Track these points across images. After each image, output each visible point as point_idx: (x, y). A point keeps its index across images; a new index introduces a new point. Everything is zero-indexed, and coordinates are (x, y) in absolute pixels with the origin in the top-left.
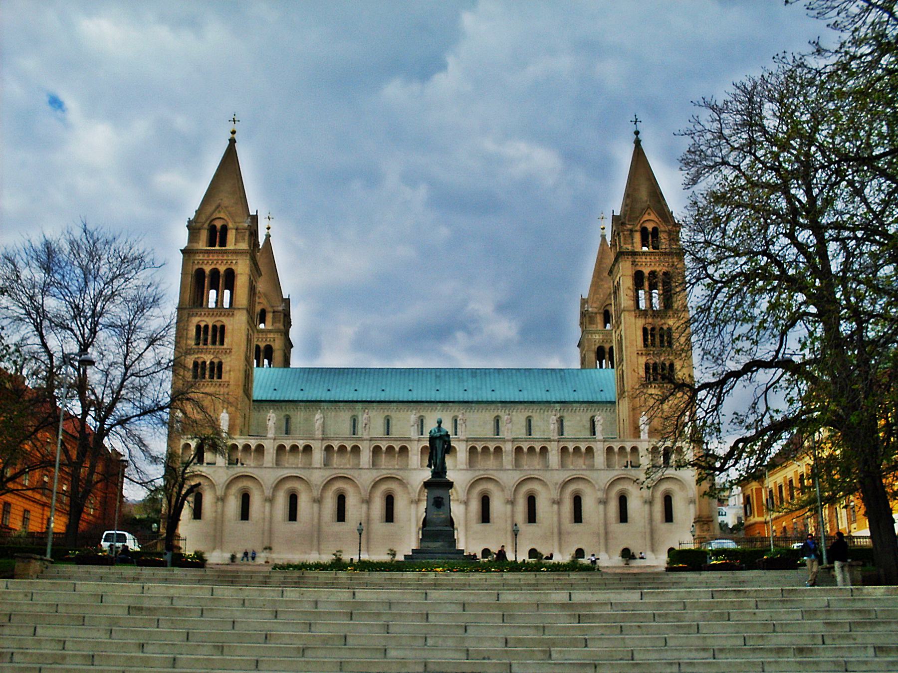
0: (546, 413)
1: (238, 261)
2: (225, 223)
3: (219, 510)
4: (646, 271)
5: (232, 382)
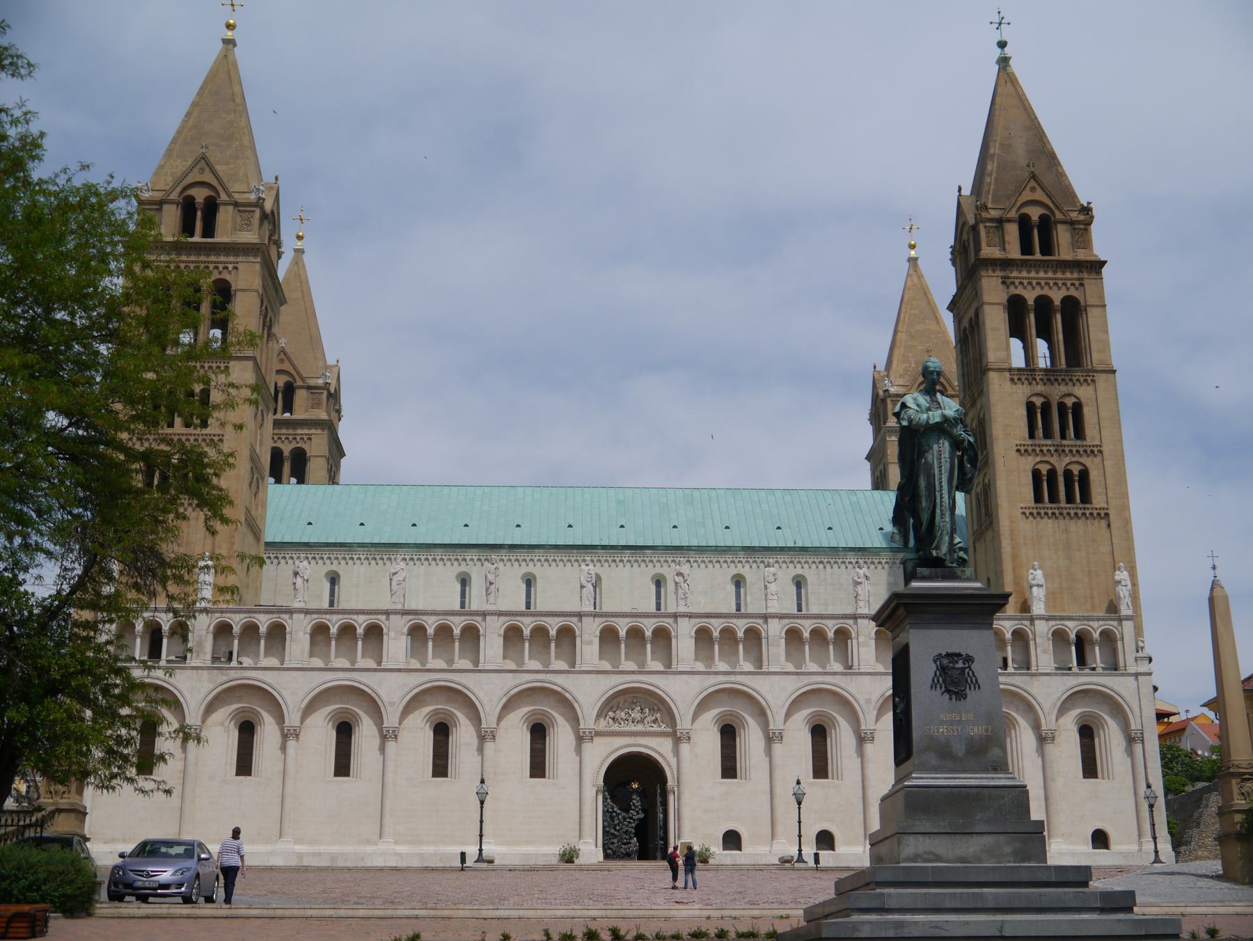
4: (1030, 296)
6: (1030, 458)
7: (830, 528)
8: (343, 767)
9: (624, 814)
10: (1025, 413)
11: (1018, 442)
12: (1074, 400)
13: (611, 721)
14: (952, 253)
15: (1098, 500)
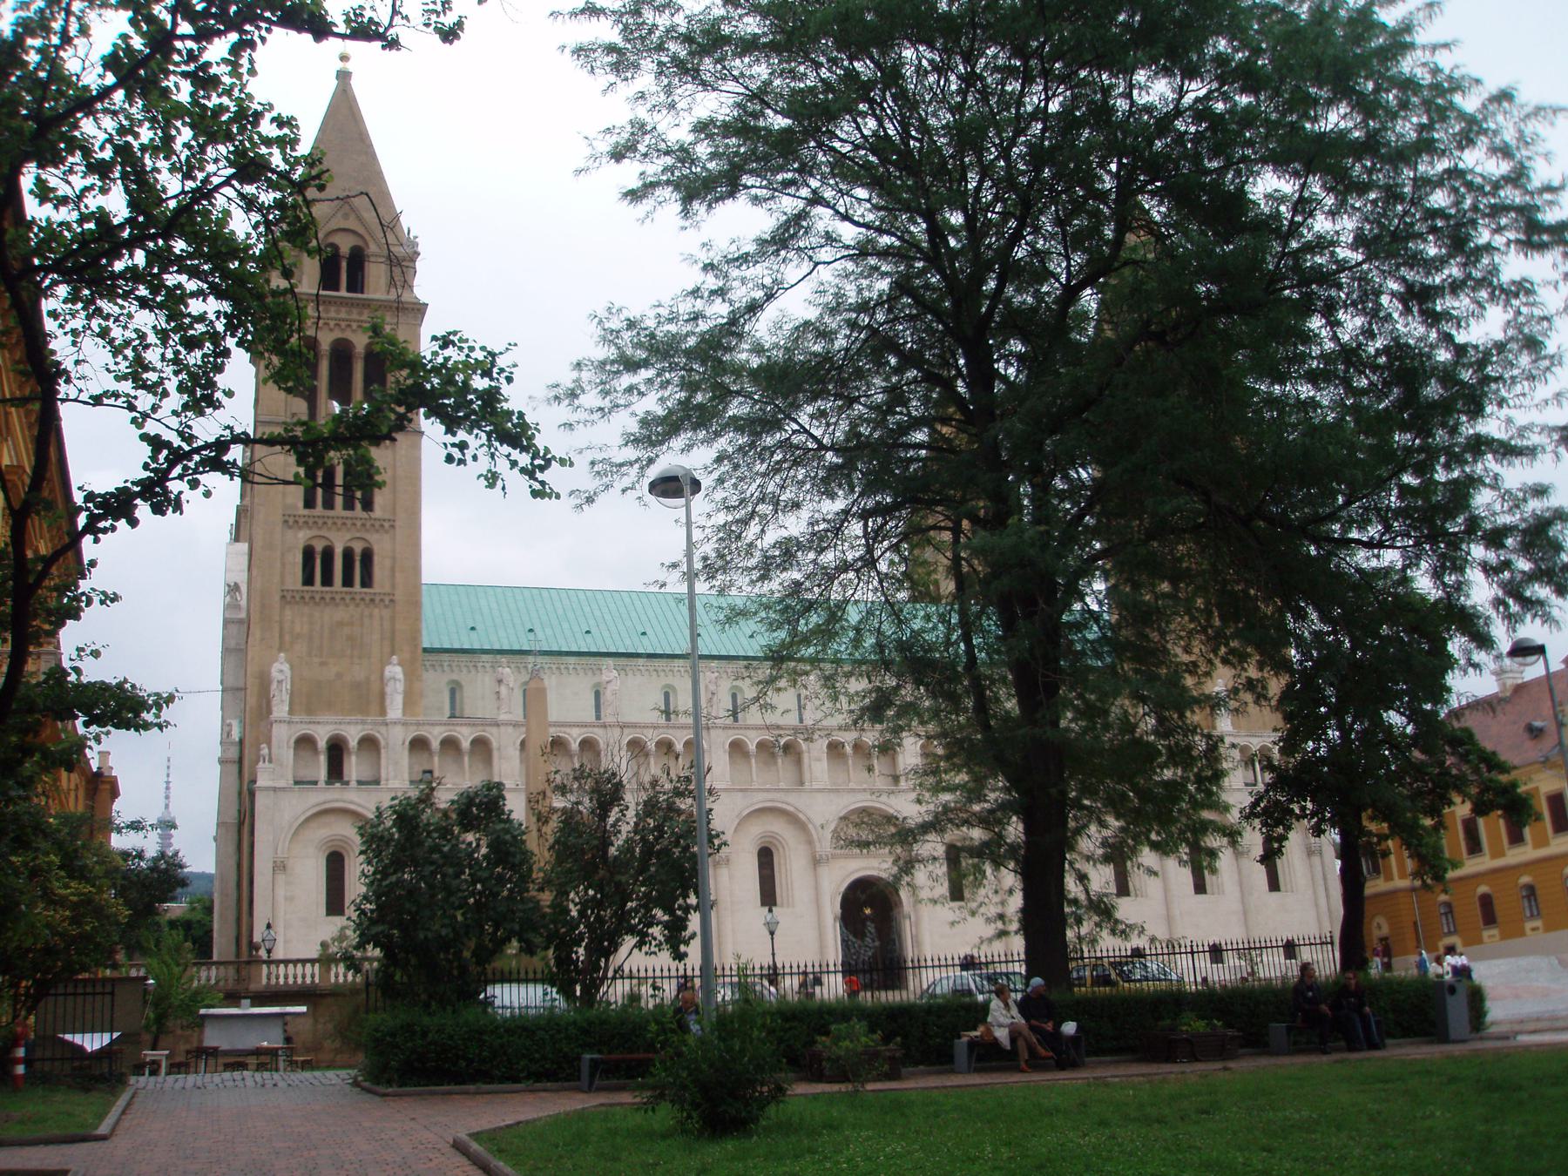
2: (360, 243)
5: (399, 596)
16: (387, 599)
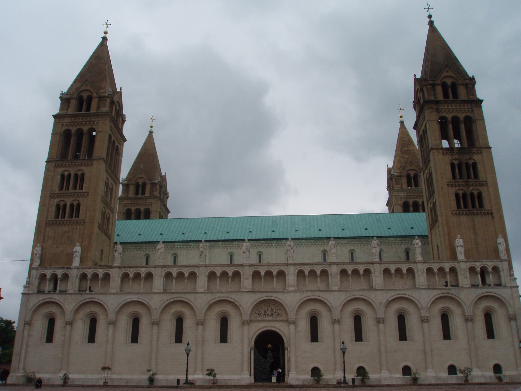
0: (366, 246)
1: (100, 122)
3: (67, 334)
4: (449, 116)
6: (454, 188)
7: (366, 229)
8: (135, 339)
9: (264, 360)
10: (450, 168)
11: (448, 181)
12: (473, 161)
13: (257, 315)
14: (414, 105)
15: (487, 205)
16: (82, 222)
